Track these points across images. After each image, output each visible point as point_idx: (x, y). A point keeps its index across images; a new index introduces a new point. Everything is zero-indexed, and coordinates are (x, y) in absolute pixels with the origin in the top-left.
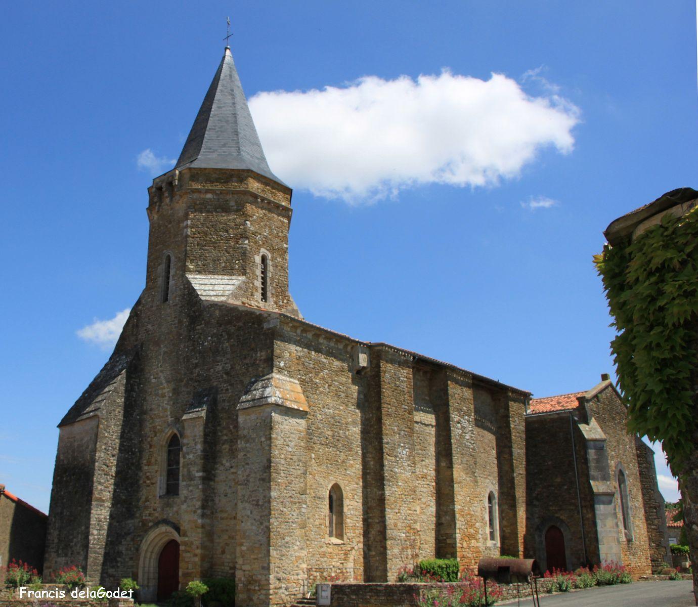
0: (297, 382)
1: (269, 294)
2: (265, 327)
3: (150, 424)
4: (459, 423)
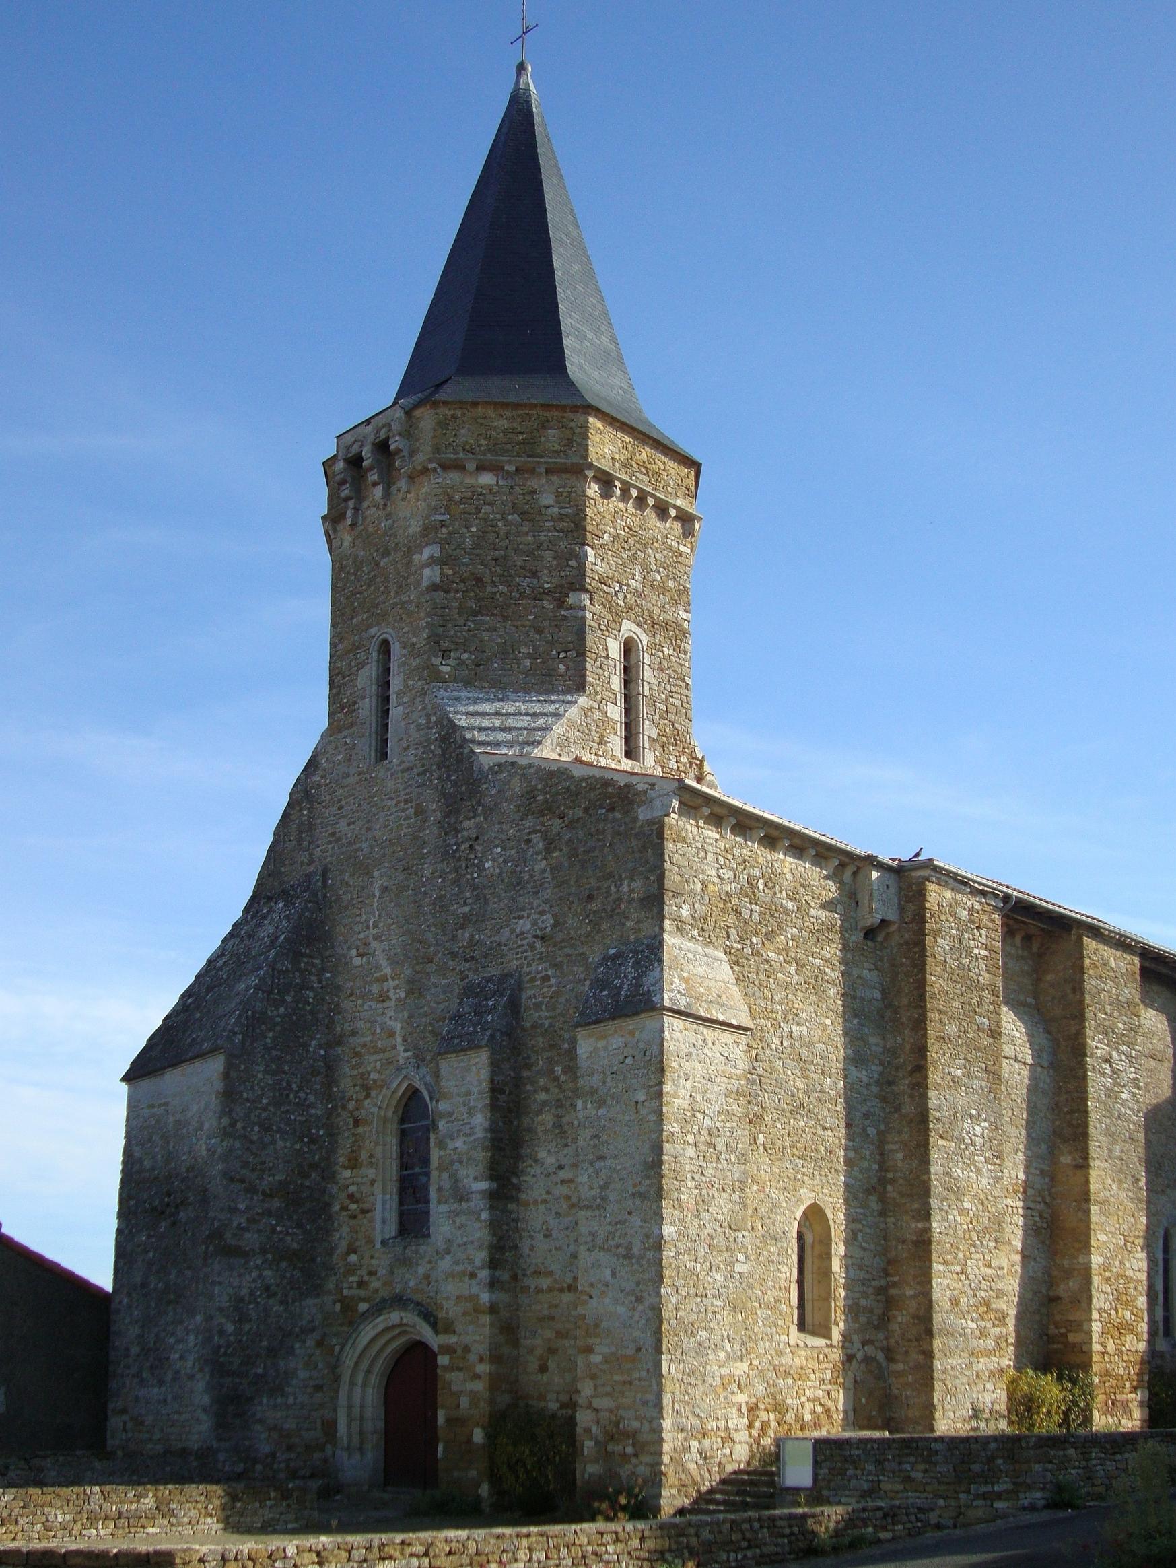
0: (721, 955)
1: (644, 741)
2: (641, 817)
3: (353, 1067)
4: (1107, 1061)
